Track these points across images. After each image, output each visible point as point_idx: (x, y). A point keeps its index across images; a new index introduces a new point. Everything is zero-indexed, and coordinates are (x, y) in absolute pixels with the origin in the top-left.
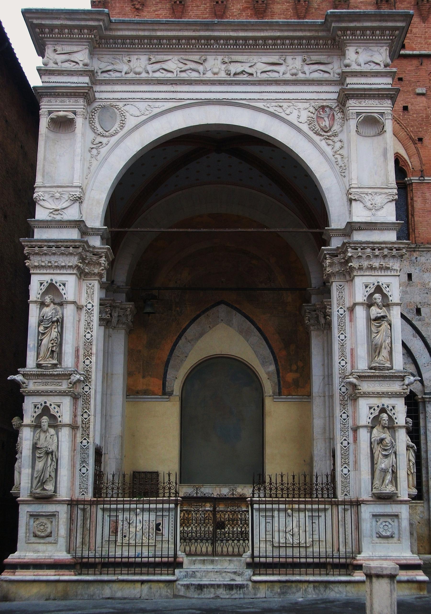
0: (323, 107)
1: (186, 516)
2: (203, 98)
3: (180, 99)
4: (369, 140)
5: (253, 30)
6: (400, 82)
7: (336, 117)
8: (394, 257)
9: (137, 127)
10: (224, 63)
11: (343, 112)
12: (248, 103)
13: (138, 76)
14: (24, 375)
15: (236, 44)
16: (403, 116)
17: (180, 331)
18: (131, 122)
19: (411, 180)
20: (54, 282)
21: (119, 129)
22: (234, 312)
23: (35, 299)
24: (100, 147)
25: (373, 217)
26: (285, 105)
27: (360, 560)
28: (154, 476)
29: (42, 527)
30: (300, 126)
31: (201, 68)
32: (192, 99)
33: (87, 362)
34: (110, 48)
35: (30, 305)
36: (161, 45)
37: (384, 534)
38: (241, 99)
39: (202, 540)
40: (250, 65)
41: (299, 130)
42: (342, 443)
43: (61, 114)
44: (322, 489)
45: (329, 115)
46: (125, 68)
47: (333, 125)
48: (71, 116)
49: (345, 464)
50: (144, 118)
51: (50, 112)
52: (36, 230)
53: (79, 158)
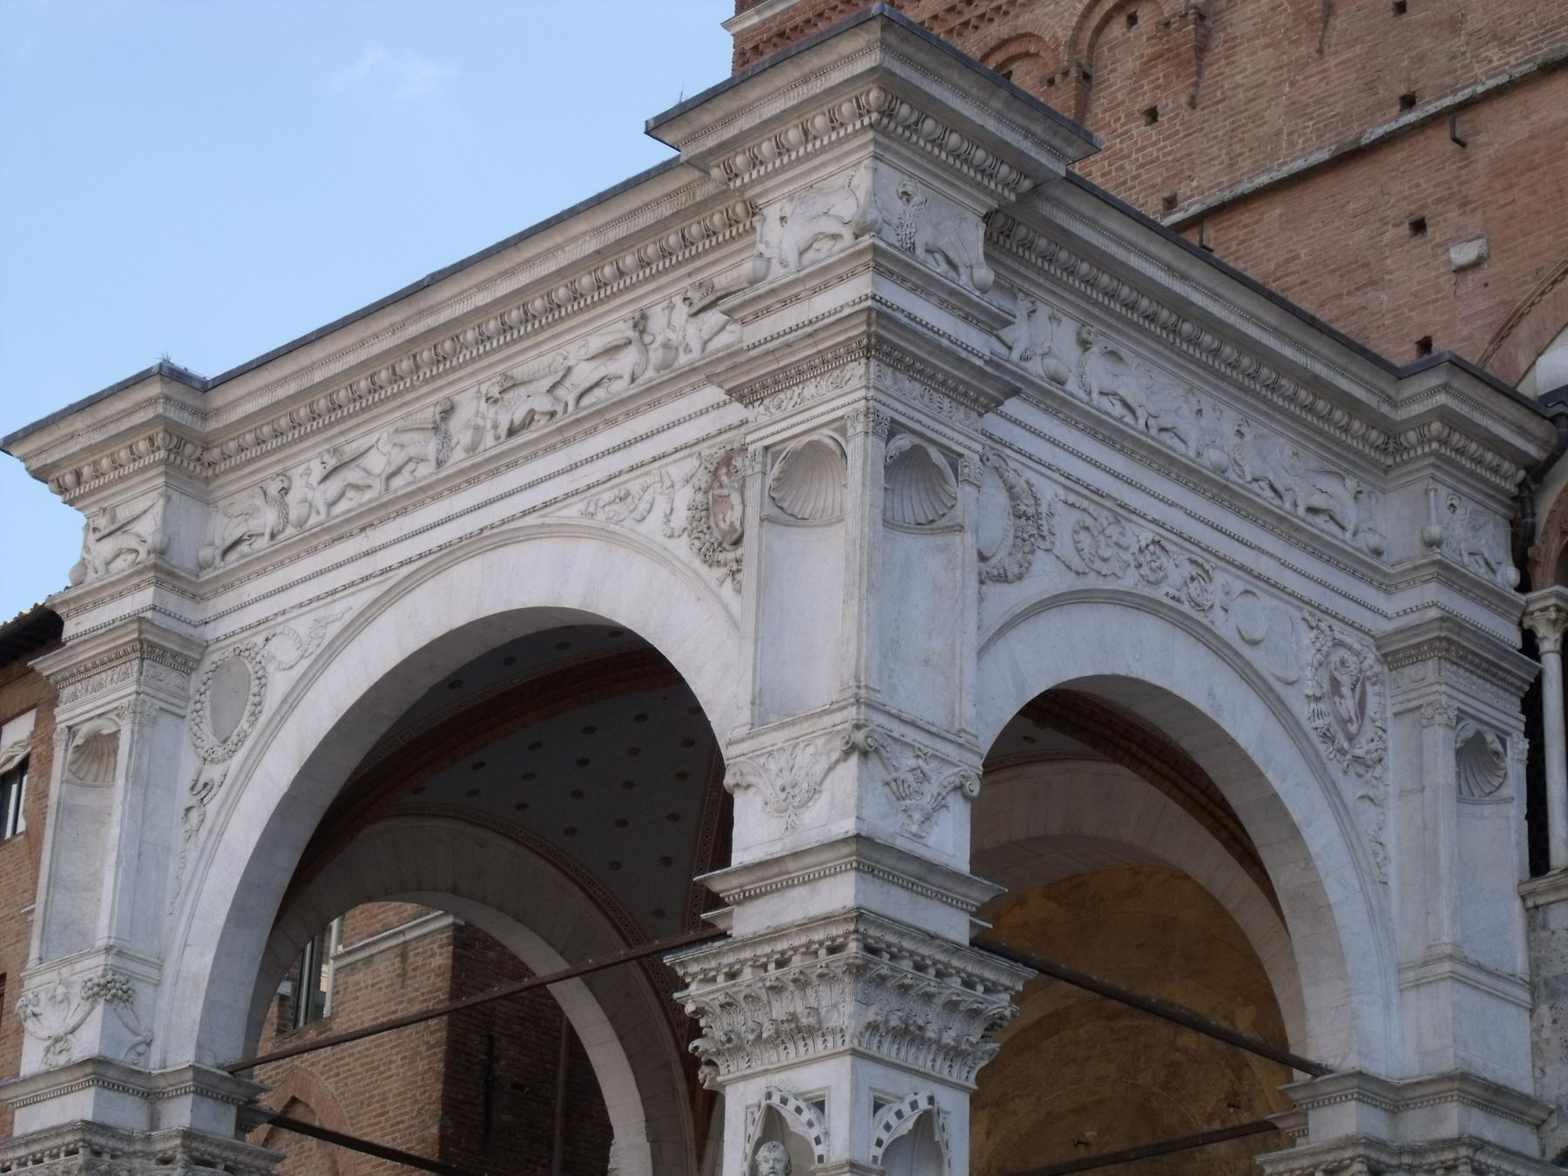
5: (528, 261)
12: (540, 521)
24: (206, 800)
26: (635, 487)
32: (410, 561)
38: (524, 514)
46: (268, 518)
50: (306, 663)
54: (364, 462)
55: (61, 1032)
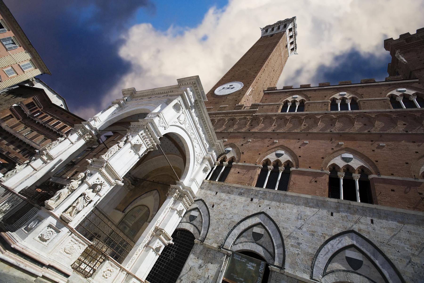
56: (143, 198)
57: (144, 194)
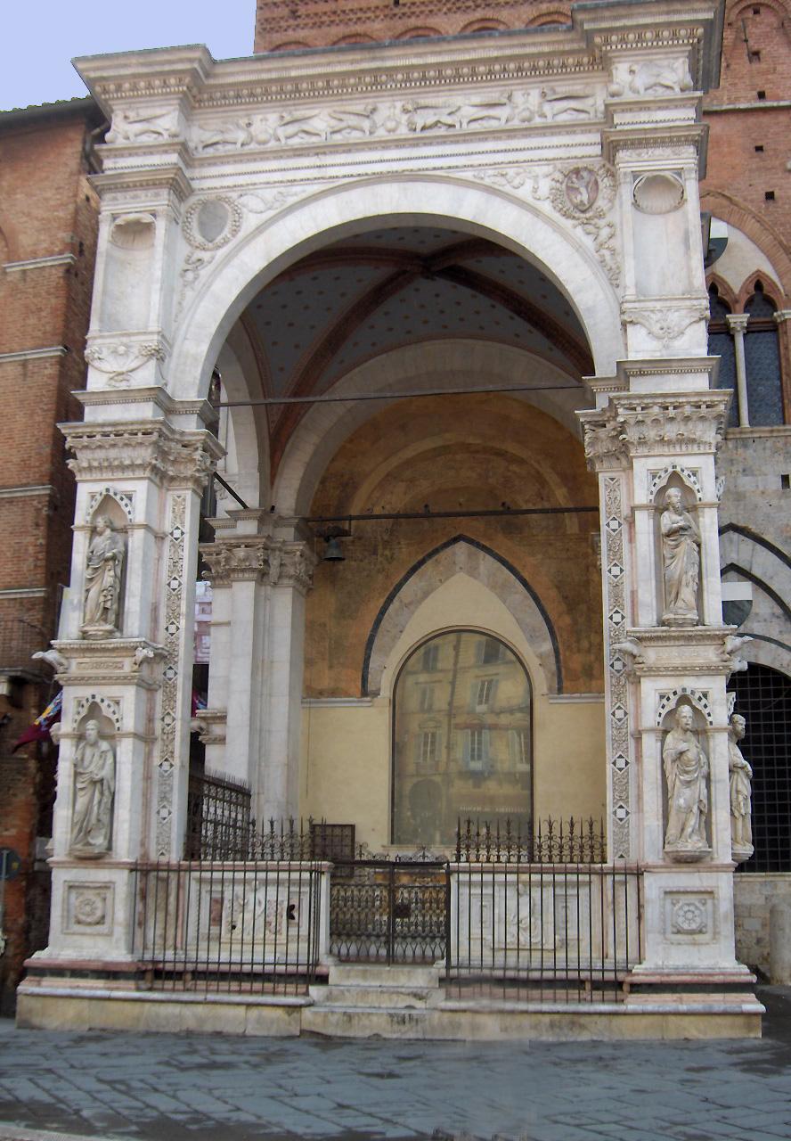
0: (577, 171)
1: (342, 893)
2: (369, 172)
3: (330, 178)
4: (660, 220)
6: (760, 153)
7: (601, 186)
8: (702, 418)
9: (260, 230)
10: (405, 111)
11: (613, 175)
13: (262, 146)
14: (60, 651)
15: (424, 78)
16: (767, 208)
17: (392, 589)
18: (250, 222)
19: (783, 315)
20: (111, 494)
21: (229, 236)
22: (482, 554)
23: (83, 523)
25: (664, 352)
26: (511, 172)
27: (638, 974)
28: (347, 832)
29: (88, 909)
30: (538, 205)
31: (366, 124)
32: (352, 176)
33: (172, 629)
34: (218, 106)
35: (75, 533)
36: (300, 92)
37: (686, 926)
38: (434, 169)
39: (424, 938)
40: (449, 111)
41: (536, 212)
42: (614, 763)
43: (132, 217)
44: (582, 847)
45: (588, 183)
46: (241, 136)
47: (595, 200)
48: (147, 218)
49: (621, 802)
50: (271, 213)
51: (114, 217)
52: (87, 410)
53: (158, 286)
54: (311, 121)
55: (124, 370)
56: (420, 601)
57: (406, 579)
